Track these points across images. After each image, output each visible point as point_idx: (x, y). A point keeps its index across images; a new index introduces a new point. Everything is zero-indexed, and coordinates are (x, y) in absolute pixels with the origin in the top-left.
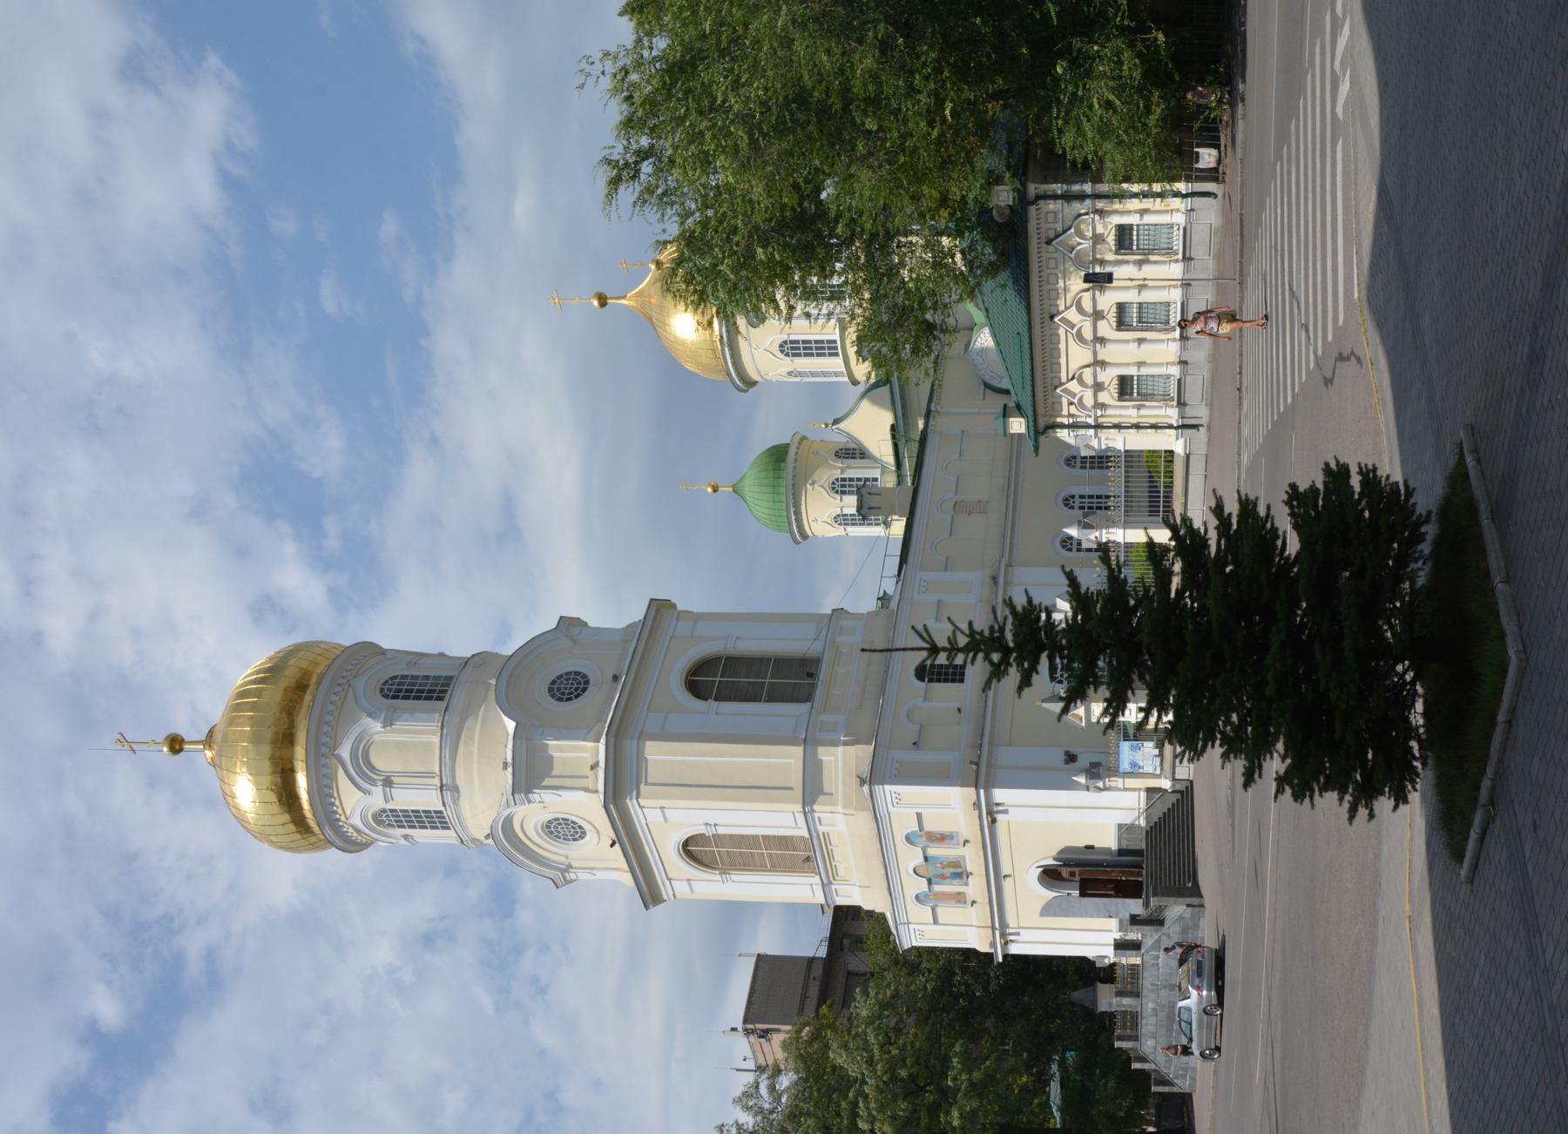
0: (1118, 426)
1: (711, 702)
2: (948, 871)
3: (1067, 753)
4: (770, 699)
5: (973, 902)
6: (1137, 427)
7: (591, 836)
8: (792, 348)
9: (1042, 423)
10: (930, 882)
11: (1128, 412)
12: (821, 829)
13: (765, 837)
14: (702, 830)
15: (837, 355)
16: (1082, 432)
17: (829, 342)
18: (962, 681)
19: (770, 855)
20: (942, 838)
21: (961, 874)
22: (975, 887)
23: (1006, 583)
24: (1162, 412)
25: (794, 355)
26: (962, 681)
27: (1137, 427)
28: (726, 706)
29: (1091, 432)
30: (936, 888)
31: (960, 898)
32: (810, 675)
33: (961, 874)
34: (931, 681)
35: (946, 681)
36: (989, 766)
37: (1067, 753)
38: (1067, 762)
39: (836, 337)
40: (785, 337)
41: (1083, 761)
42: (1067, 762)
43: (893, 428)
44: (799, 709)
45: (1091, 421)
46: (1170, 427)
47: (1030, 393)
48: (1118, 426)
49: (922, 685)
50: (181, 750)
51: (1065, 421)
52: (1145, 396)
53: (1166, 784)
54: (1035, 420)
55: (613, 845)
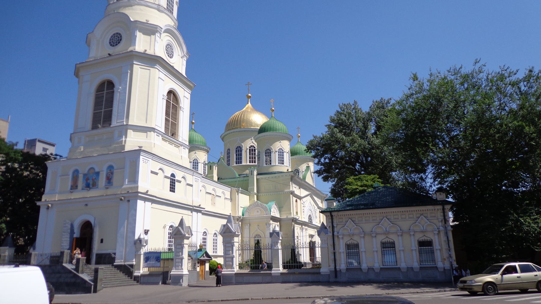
1: (166, 98)
2: (91, 182)
3: (148, 231)
4: (166, 119)
6: (335, 253)
8: (239, 150)
9: (333, 214)
11: (341, 248)
19: (101, 112)
20: (109, 180)
27: (335, 253)
28: (165, 102)
31: (74, 187)
32: (172, 135)
34: (171, 179)
37: (148, 231)
38: (145, 230)
41: (146, 237)
42: (145, 230)
44: (163, 130)
45: (335, 233)
49: (169, 176)
52: (349, 255)
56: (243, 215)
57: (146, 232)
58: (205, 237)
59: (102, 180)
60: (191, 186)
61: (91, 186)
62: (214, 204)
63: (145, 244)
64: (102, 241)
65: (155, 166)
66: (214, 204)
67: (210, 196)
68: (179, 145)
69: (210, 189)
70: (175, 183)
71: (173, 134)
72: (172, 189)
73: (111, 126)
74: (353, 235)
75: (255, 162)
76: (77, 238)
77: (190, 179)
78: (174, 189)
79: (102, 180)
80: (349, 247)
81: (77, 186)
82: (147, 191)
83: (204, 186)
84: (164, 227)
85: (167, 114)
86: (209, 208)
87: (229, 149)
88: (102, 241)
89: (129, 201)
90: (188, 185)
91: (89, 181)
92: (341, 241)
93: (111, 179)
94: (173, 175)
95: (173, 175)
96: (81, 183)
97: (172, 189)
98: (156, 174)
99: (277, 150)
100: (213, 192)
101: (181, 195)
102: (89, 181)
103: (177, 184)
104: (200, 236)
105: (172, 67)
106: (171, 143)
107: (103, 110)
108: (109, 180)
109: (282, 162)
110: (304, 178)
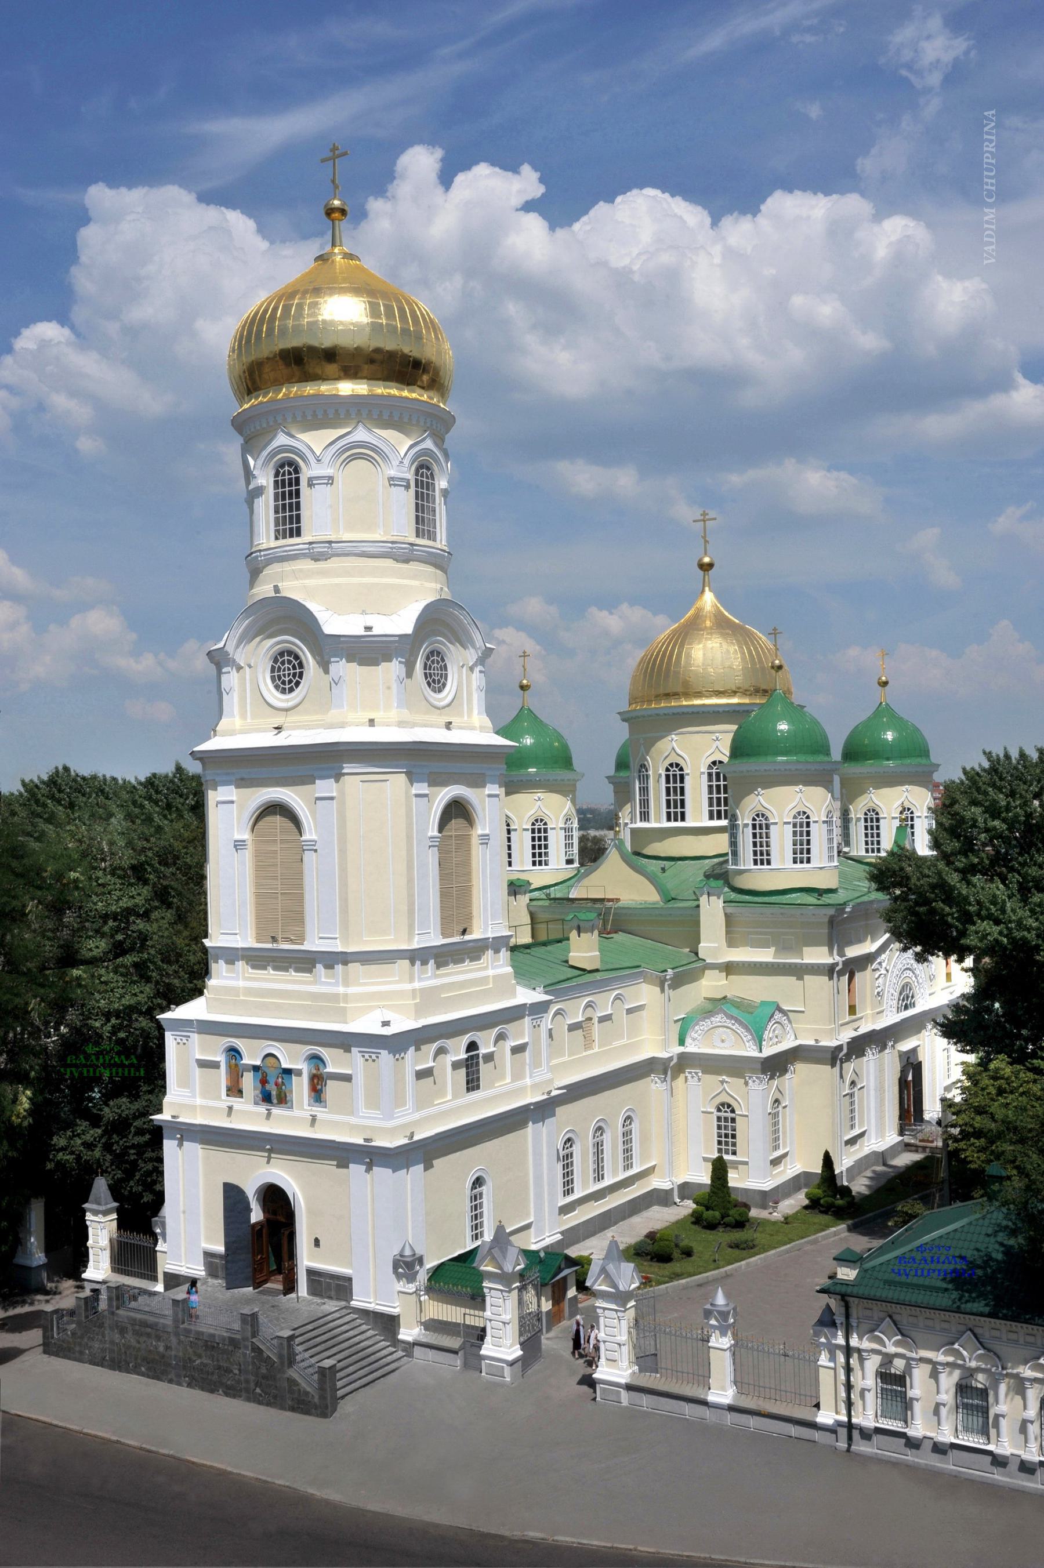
0: (848, 1370)
6: (849, 1387)
25: (668, 777)
39: (688, 823)
40: (686, 771)
48: (848, 1370)
80: (885, 1376)
88: (317, 1243)
91: (268, 1087)
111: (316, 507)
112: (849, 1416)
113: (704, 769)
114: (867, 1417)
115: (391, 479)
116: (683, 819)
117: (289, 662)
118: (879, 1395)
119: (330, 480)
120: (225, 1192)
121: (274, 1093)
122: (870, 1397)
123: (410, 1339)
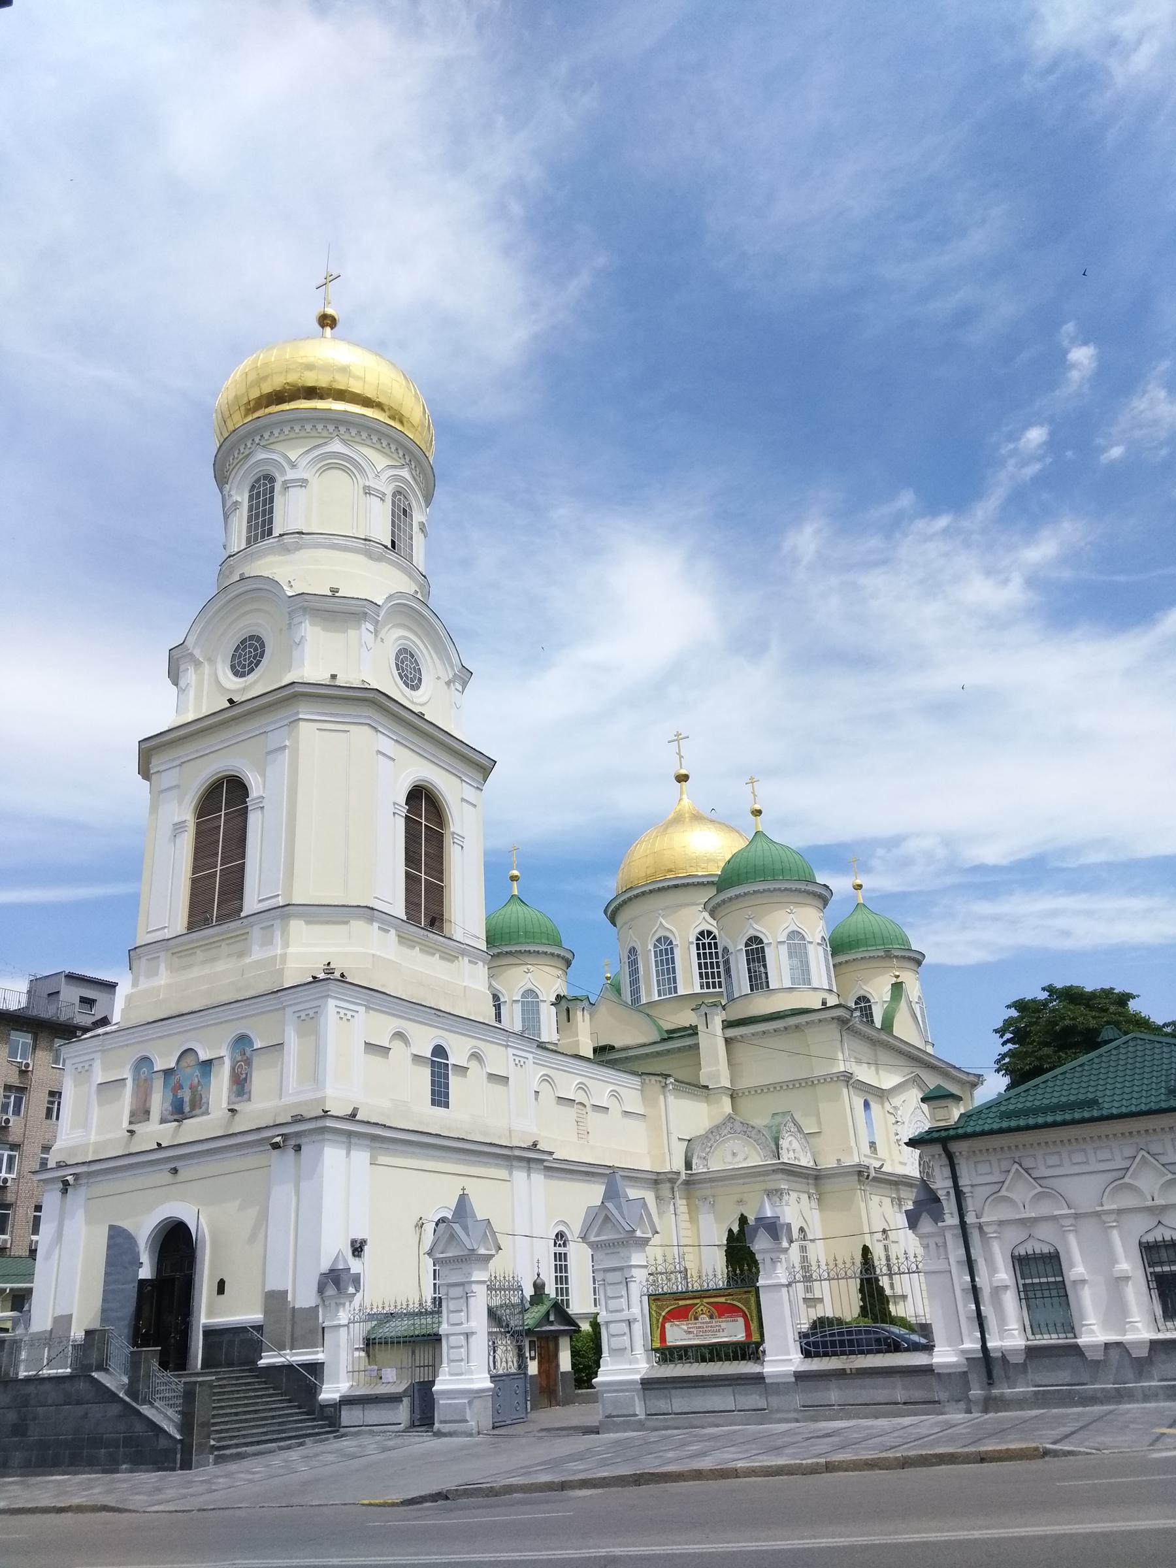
1: (404, 810)
2: (186, 1095)
3: (363, 1243)
4: (407, 874)
5: (131, 1132)
6: (975, 1291)
7: (232, 683)
8: (665, 950)
9: (955, 1147)
10: (168, 1072)
12: (256, 932)
13: (242, 868)
14: (254, 793)
15: (660, 995)
16: (949, 1206)
17: (675, 988)
18: (434, 1103)
20: (240, 1084)
21: (179, 1112)
22: (155, 1131)
23: (529, 1160)
24: (1013, 1324)
26: (434, 1103)
29: (952, 1220)
30: (158, 1083)
31: (141, 1113)
33: (179, 1112)
35: (433, 1082)
36: (350, 1134)
37: (363, 1243)
38: (353, 1242)
41: (355, 1266)
42: (353, 1242)
43: (612, 1048)
44: (400, 910)
45: (970, 1219)
46: (984, 1340)
47: (996, 1126)
49: (428, 1053)
50: (323, 326)
51: (962, 1182)
53: (330, 1392)
54: (966, 1136)
55: (231, 701)
56: (688, 1165)
57: (358, 1249)
58: (562, 1250)
59: (220, 1086)
60: (504, 1080)
61: (187, 1109)
62: (583, 1133)
63: (351, 1290)
64: (221, 1287)
65: (381, 1027)
66: (583, 1133)
67: (571, 1112)
68: (455, 952)
69: (568, 1085)
70: (447, 1077)
71: (436, 921)
72: (440, 1097)
73: (243, 914)
74: (1035, 1221)
75: (720, 987)
76: (142, 1282)
77: (499, 1058)
78: (447, 1095)
79: (220, 1086)
80: (1022, 1263)
81: (148, 1112)
82: (356, 1110)
83: (546, 1079)
84: (420, 1225)
85: (411, 858)
86: (567, 1149)
87: (633, 951)
88: (221, 1287)
89: (298, 1148)
90: (492, 1077)
92: (996, 1247)
93: (245, 1079)
94: (439, 1051)
95: (439, 1051)
96: (158, 1102)
97: (440, 1097)
98: (384, 1051)
99: (783, 938)
100: (580, 1097)
101: (473, 1109)
102: (180, 1094)
103: (454, 1081)
104: (546, 1252)
105: (420, 716)
106: (428, 949)
107: (218, 869)
108: (240, 1084)
109: (803, 975)
110: (888, 1025)
111: (290, 512)
112: (984, 1340)
113: (693, 939)
114: (1010, 1334)
115: (365, 487)
116: (676, 992)
117: (251, 646)
118: (1022, 1294)
119: (303, 483)
120: (110, 1237)
121: (187, 1099)
122: (1010, 1300)
123: (336, 1396)
